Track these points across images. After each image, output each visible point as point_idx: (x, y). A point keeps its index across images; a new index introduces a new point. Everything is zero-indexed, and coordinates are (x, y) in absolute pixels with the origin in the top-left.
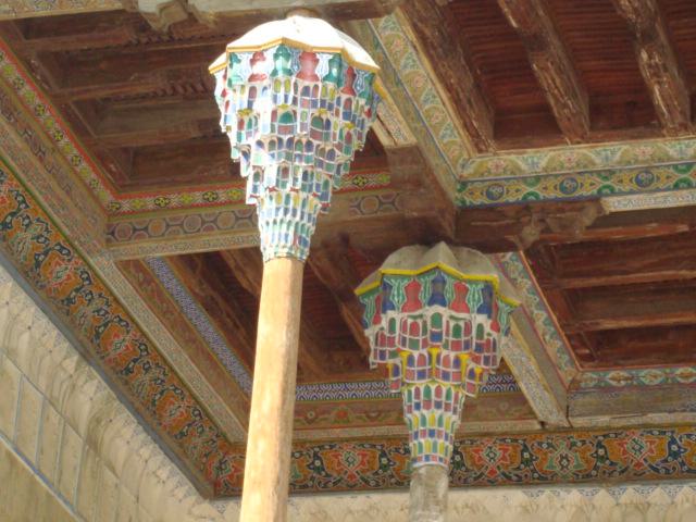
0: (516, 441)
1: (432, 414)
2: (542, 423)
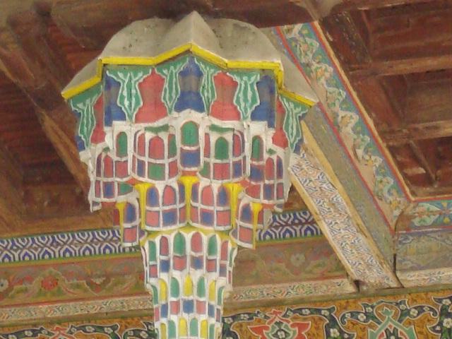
0: (319, 311)
1: (187, 278)
2: (357, 283)
